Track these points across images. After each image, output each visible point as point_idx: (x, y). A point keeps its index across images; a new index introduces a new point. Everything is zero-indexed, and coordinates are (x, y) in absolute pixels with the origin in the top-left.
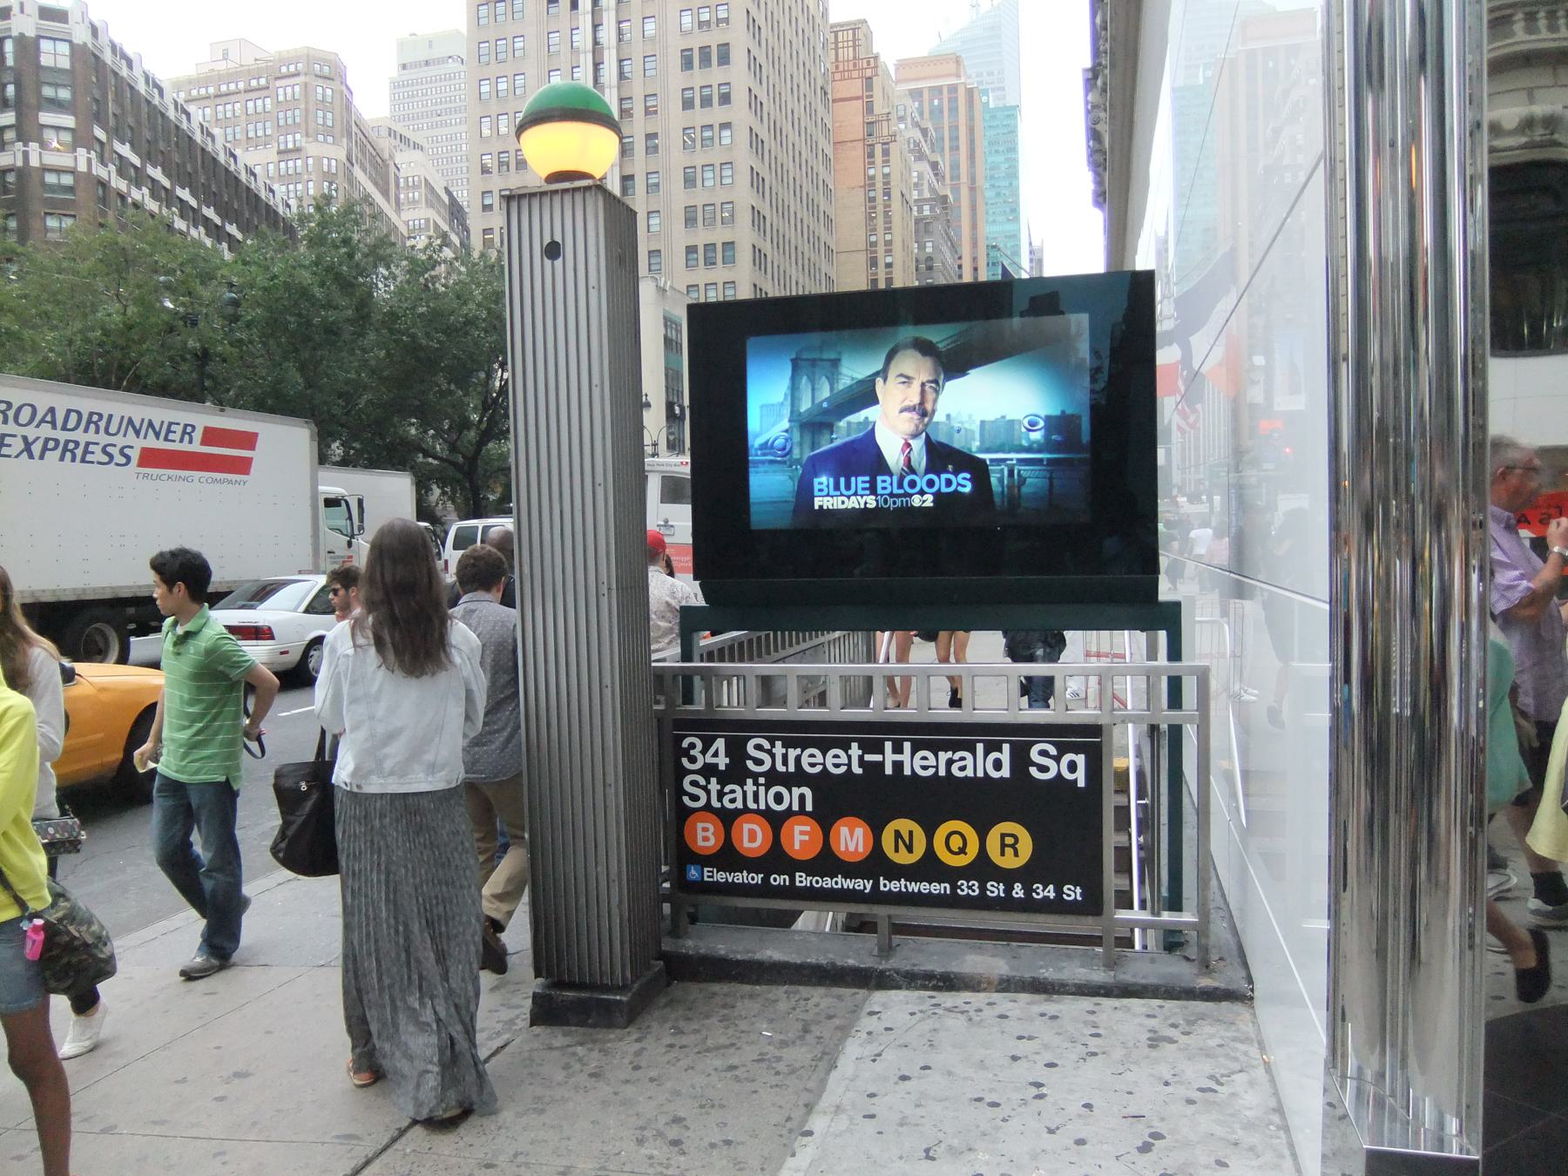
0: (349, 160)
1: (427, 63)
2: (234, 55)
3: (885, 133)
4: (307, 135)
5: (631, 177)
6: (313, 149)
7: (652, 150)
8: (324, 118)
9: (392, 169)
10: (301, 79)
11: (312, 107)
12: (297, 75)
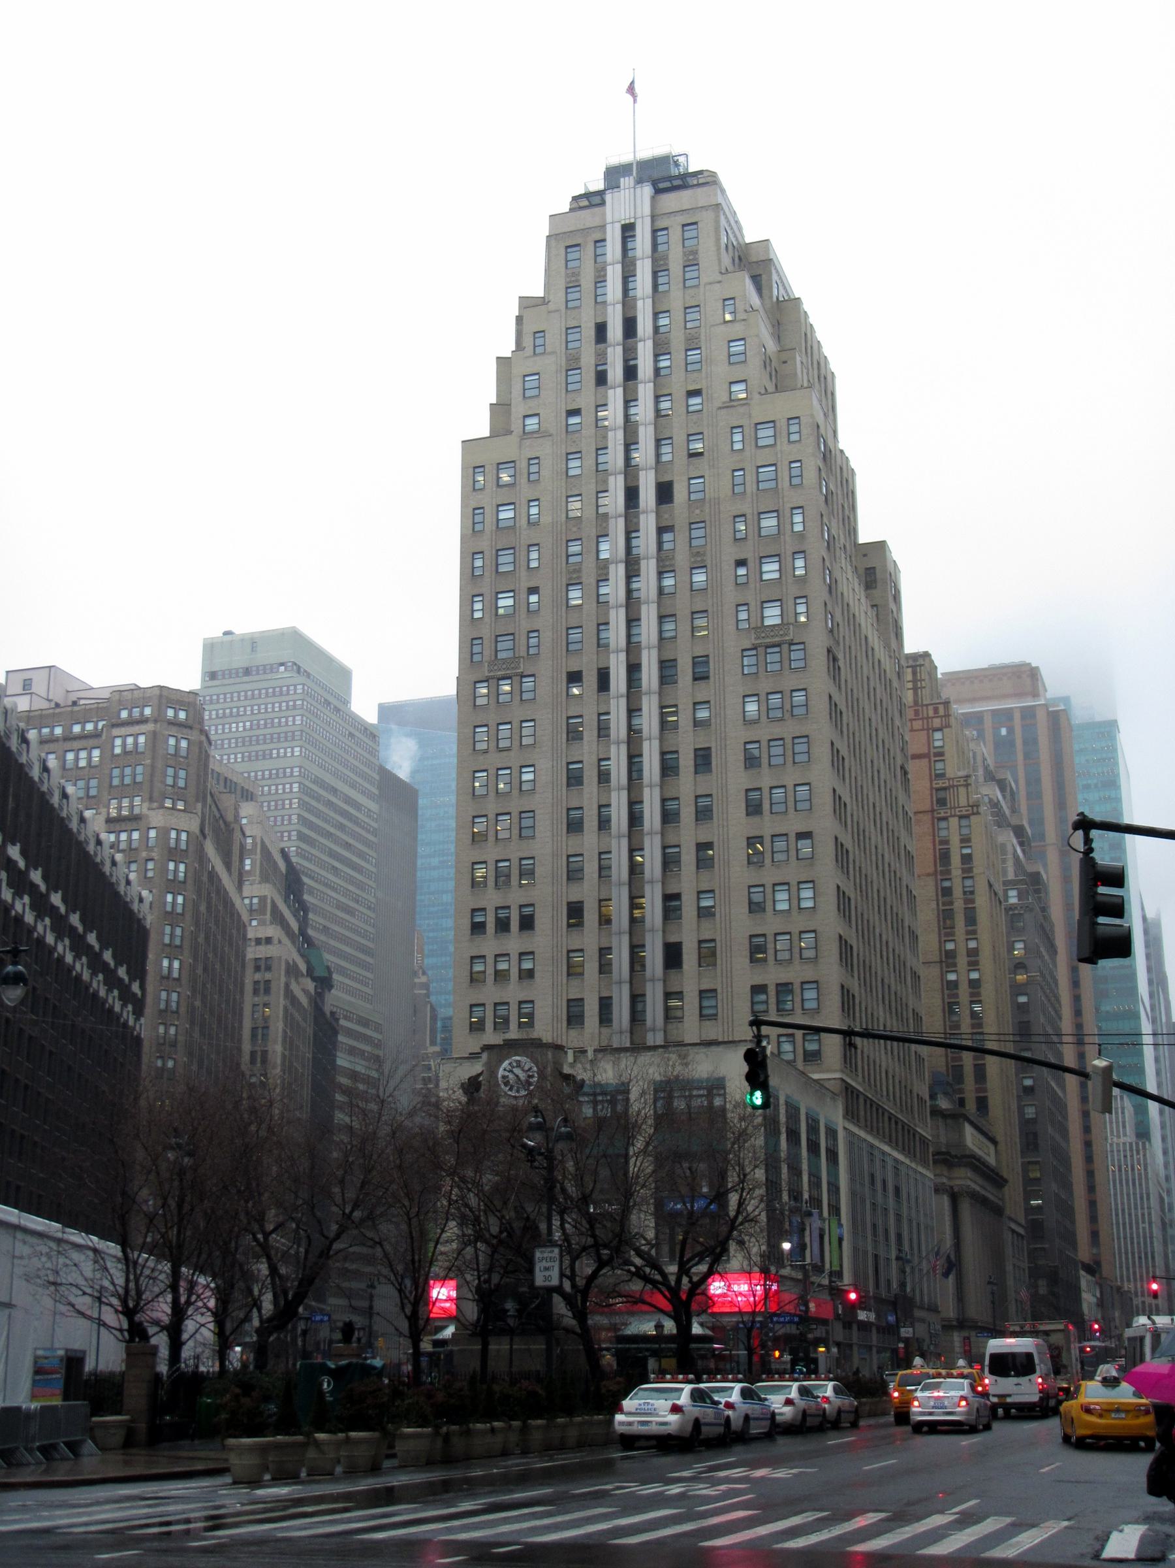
0: (202, 831)
1: (247, 671)
2: (39, 687)
3: (963, 801)
4: (151, 800)
5: (677, 897)
6: (157, 818)
7: (703, 862)
8: (175, 777)
9: (237, 835)
10: (150, 727)
11: (159, 765)
12: (143, 721)
